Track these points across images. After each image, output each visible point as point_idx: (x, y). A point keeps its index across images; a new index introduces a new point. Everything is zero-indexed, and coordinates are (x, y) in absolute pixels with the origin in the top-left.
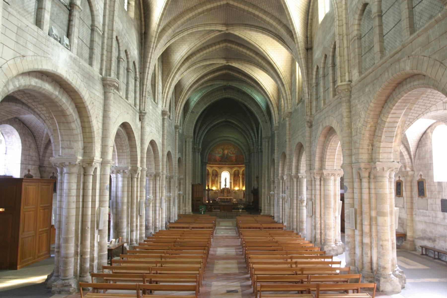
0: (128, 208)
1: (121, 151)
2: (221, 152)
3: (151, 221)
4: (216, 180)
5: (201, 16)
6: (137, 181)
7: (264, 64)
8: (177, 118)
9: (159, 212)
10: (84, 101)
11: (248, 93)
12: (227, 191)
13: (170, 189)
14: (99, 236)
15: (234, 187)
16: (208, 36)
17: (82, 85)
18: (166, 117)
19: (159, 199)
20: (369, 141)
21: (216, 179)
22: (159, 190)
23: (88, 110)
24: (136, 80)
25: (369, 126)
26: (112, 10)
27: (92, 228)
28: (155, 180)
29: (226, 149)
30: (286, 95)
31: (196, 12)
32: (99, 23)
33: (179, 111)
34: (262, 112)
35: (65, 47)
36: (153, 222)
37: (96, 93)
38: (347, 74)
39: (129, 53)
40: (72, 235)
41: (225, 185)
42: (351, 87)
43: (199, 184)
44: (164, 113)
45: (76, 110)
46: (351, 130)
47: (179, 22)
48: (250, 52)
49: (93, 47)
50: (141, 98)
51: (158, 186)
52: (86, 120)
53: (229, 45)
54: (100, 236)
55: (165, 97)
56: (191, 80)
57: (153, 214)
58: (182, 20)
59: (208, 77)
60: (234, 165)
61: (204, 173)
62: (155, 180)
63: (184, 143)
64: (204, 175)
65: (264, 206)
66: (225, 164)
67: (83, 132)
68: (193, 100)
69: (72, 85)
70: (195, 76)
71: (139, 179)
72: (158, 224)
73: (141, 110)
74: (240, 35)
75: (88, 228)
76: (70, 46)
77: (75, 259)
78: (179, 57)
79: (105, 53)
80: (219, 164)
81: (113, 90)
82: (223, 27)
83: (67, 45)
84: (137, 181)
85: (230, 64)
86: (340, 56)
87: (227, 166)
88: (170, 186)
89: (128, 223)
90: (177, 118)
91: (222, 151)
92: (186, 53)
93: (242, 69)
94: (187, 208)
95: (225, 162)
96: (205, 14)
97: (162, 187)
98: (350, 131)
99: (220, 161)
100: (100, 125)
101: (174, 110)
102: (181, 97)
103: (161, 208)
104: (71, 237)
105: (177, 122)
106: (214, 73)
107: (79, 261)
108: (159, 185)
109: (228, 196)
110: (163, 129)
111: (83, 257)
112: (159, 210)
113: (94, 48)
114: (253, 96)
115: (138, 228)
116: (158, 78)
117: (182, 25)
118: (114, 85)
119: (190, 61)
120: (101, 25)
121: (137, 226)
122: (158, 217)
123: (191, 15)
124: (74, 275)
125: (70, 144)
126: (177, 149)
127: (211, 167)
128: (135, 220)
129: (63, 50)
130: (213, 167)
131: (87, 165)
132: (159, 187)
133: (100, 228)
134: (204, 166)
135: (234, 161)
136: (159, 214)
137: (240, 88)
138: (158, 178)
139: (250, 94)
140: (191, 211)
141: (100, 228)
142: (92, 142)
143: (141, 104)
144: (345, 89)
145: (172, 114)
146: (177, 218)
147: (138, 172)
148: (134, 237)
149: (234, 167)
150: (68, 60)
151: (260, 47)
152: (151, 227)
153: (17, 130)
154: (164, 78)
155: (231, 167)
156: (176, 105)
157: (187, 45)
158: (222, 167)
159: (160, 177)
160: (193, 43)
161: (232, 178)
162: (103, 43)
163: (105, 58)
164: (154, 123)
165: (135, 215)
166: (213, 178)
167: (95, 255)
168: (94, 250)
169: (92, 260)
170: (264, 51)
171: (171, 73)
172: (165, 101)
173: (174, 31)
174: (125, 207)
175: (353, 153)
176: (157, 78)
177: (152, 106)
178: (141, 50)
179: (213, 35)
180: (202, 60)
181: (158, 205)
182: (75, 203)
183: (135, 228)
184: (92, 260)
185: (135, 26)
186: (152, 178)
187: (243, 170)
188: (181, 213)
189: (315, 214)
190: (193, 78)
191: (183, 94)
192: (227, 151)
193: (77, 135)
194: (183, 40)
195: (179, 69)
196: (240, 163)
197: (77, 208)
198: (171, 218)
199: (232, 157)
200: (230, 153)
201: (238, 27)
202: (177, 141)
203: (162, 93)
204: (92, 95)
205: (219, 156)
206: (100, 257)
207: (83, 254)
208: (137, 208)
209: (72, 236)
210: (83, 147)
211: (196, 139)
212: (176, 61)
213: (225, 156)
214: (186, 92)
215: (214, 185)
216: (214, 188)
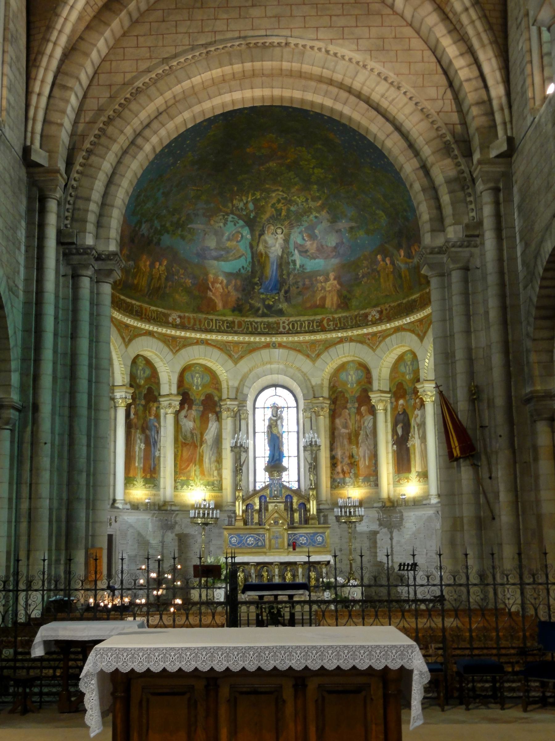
2: (243, 247)
4: (210, 435)
12: (290, 509)
15: (336, 484)
21: (213, 427)
29: (276, 219)
61: (84, 344)
64: (84, 360)
66: (272, 330)
80: (230, 329)
87: (284, 339)
91: (246, 232)
95: (271, 311)
109: (294, 546)
130: (186, 343)
134: (86, 283)
135: (331, 300)
149: (329, 345)
155: (313, 343)
158: (252, 349)
161: (323, 421)
166: (188, 425)
187: (401, 359)
192: (280, 237)
196: (374, 313)
199: (313, 275)
200: (304, 252)
205: (229, 275)
213: (271, 271)
215: (194, 470)
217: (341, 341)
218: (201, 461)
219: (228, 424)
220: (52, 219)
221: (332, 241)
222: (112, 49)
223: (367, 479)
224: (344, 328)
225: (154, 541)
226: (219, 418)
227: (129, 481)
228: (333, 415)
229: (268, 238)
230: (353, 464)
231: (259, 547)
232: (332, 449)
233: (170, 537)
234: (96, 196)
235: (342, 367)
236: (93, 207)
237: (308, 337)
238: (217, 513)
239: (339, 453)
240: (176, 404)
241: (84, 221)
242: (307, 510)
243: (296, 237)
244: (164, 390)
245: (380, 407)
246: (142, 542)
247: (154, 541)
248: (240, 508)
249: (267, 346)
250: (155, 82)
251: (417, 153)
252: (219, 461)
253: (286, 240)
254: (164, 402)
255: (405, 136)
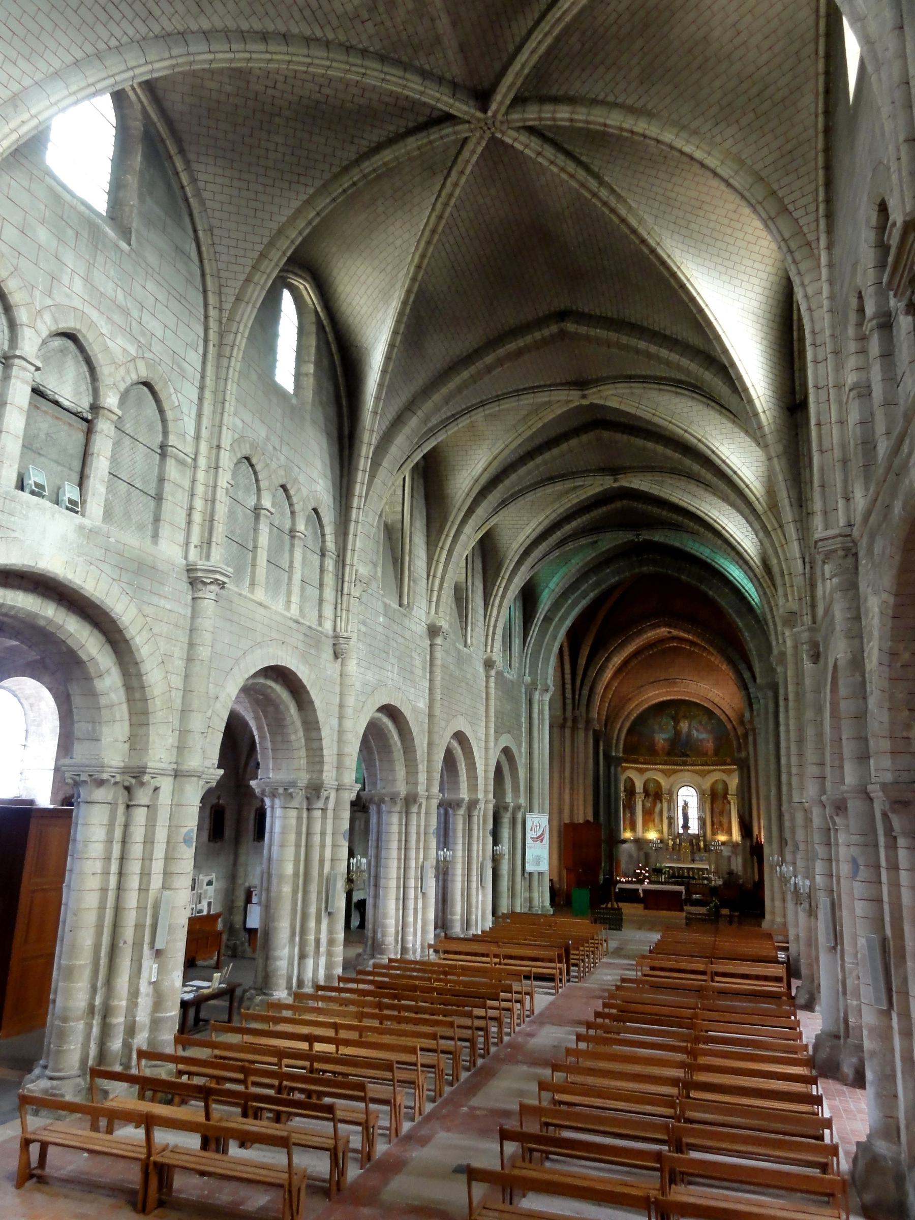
0: (295, 892)
1: (279, 738)
2: (670, 728)
3: (391, 930)
5: (495, 373)
6: (324, 818)
7: (708, 476)
8: (490, 638)
9: (416, 904)
10: (122, 627)
11: (704, 558)
13: (470, 837)
14: (156, 966)
15: (714, 833)
16: (537, 418)
17: (116, 590)
18: (439, 640)
19: (416, 868)
20: (907, 713)
21: (658, 806)
22: (418, 841)
23: (134, 648)
24: (323, 555)
25: (899, 664)
26: (220, 399)
27: (138, 945)
28: (407, 813)
29: (685, 717)
30: (779, 563)
31: (480, 365)
32: (183, 435)
33: (496, 621)
34: (750, 608)
35: (67, 508)
36: (397, 932)
37: (162, 602)
38: (841, 503)
39: (292, 492)
40: (84, 960)
41: (686, 826)
42: (853, 542)
43: (587, 822)
44: (433, 631)
45: (108, 647)
46: (863, 676)
47: (437, 397)
48: (666, 446)
49: (162, 494)
50: (339, 601)
51: (413, 829)
52: (132, 670)
53: (606, 434)
54: (159, 967)
55: (436, 588)
56: (522, 534)
57: (397, 909)
58: (444, 391)
59: (574, 524)
60: (712, 765)
62: (407, 813)
63: (524, 707)
65: (773, 900)
66: (685, 764)
67: (128, 701)
68: (547, 586)
69: (82, 592)
70: (534, 524)
71: (330, 814)
72: (410, 938)
73: (338, 629)
74: (623, 407)
75: (125, 942)
76: (84, 502)
77: (86, 1024)
78: (467, 482)
79: (199, 504)
80: (665, 763)
81: (210, 592)
82: (572, 392)
83: (71, 501)
84: (324, 818)
85: (626, 484)
86: (821, 451)
87: (690, 768)
88: (470, 830)
89: (293, 934)
90: (490, 638)
92: (485, 470)
93: (662, 495)
94: (536, 895)
96: (505, 366)
97: (425, 834)
98: (860, 679)
99: (669, 754)
100: (177, 681)
101: (482, 619)
102: (498, 584)
103: (424, 894)
104: (80, 966)
105: (489, 650)
106: (588, 512)
107: (96, 1030)
108: (418, 826)
109: (693, 861)
110: (431, 673)
111: (108, 1020)
112: (416, 898)
113: (165, 496)
114: (717, 566)
115: (323, 949)
116: (411, 540)
117: (447, 403)
118: (217, 580)
119: (501, 487)
120: (189, 439)
121: (318, 942)
122: (411, 919)
123: (465, 374)
124: (80, 1069)
125: (94, 730)
126: (492, 725)
127: (641, 771)
128: (312, 924)
129: (57, 516)
131: (133, 781)
132: (418, 834)
133: (158, 946)
135: (711, 752)
136: (416, 910)
137: (677, 544)
138: (414, 809)
139: (709, 561)
140: (547, 903)
141: (158, 946)
142: (148, 724)
143: (339, 614)
144: (835, 551)
145: (472, 630)
146: (489, 924)
147: (324, 794)
148: (309, 975)
150: (72, 535)
151: (686, 431)
152: (391, 947)
153: (50, 690)
154: (433, 537)
156: (486, 605)
157: (485, 447)
158: (675, 772)
159: (420, 805)
160: (501, 442)
161: (708, 806)
162: (194, 481)
163: (197, 517)
164: (393, 660)
165: (313, 910)
166: (648, 805)
167: (137, 1019)
168: (136, 1005)
169: (131, 1030)
170: (699, 440)
171: (449, 524)
172: (434, 599)
173: (425, 422)
174: (287, 889)
175: (871, 752)
176: (407, 541)
177: (385, 615)
178: (341, 476)
179: (549, 416)
180: (542, 481)
181: (412, 883)
182: (98, 877)
183: (311, 949)
184: (131, 1030)
185: (314, 422)
186: (397, 808)
188: (518, 910)
189: (842, 944)
190: (528, 528)
191: (506, 573)
192: (687, 724)
193: (111, 706)
194: (474, 434)
195: (471, 511)
196: (729, 760)
197: (104, 890)
198: (473, 922)
199: (701, 741)
200: (697, 730)
201: (612, 386)
202: (492, 702)
203: (428, 579)
204: (149, 610)
205: (664, 739)
206: (155, 1024)
207: (107, 1012)
208: (319, 893)
209: (82, 962)
210: (128, 734)
211: (577, 692)
212: (461, 492)
213: (684, 737)
214: (511, 568)
215: (651, 825)
216: (652, 835)
217: (715, 770)
218: (654, 820)
219: (665, 805)
220: (601, 748)
221: (709, 728)
222: (619, 684)
223: (727, 833)
224: (716, 765)
225: (635, 855)
226: (661, 802)
227: (625, 830)
228: (712, 803)
229: (682, 724)
230: (721, 824)
231: (679, 860)
232: (712, 817)
233: (642, 853)
234: (615, 737)
235: (716, 781)
236: (614, 741)
237: (700, 767)
238: (661, 845)
239: (715, 820)
240: (643, 797)
241: (611, 747)
242: (699, 846)
243: (694, 723)
244: (637, 791)
245: (732, 802)
246: (630, 856)
247: (635, 855)
248: (671, 843)
249: (682, 770)
250: (635, 696)
251: (731, 722)
252: (662, 821)
253: (690, 725)
254: (637, 796)
255: (727, 715)
